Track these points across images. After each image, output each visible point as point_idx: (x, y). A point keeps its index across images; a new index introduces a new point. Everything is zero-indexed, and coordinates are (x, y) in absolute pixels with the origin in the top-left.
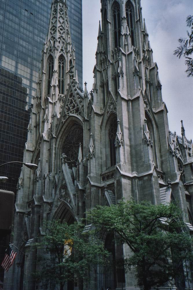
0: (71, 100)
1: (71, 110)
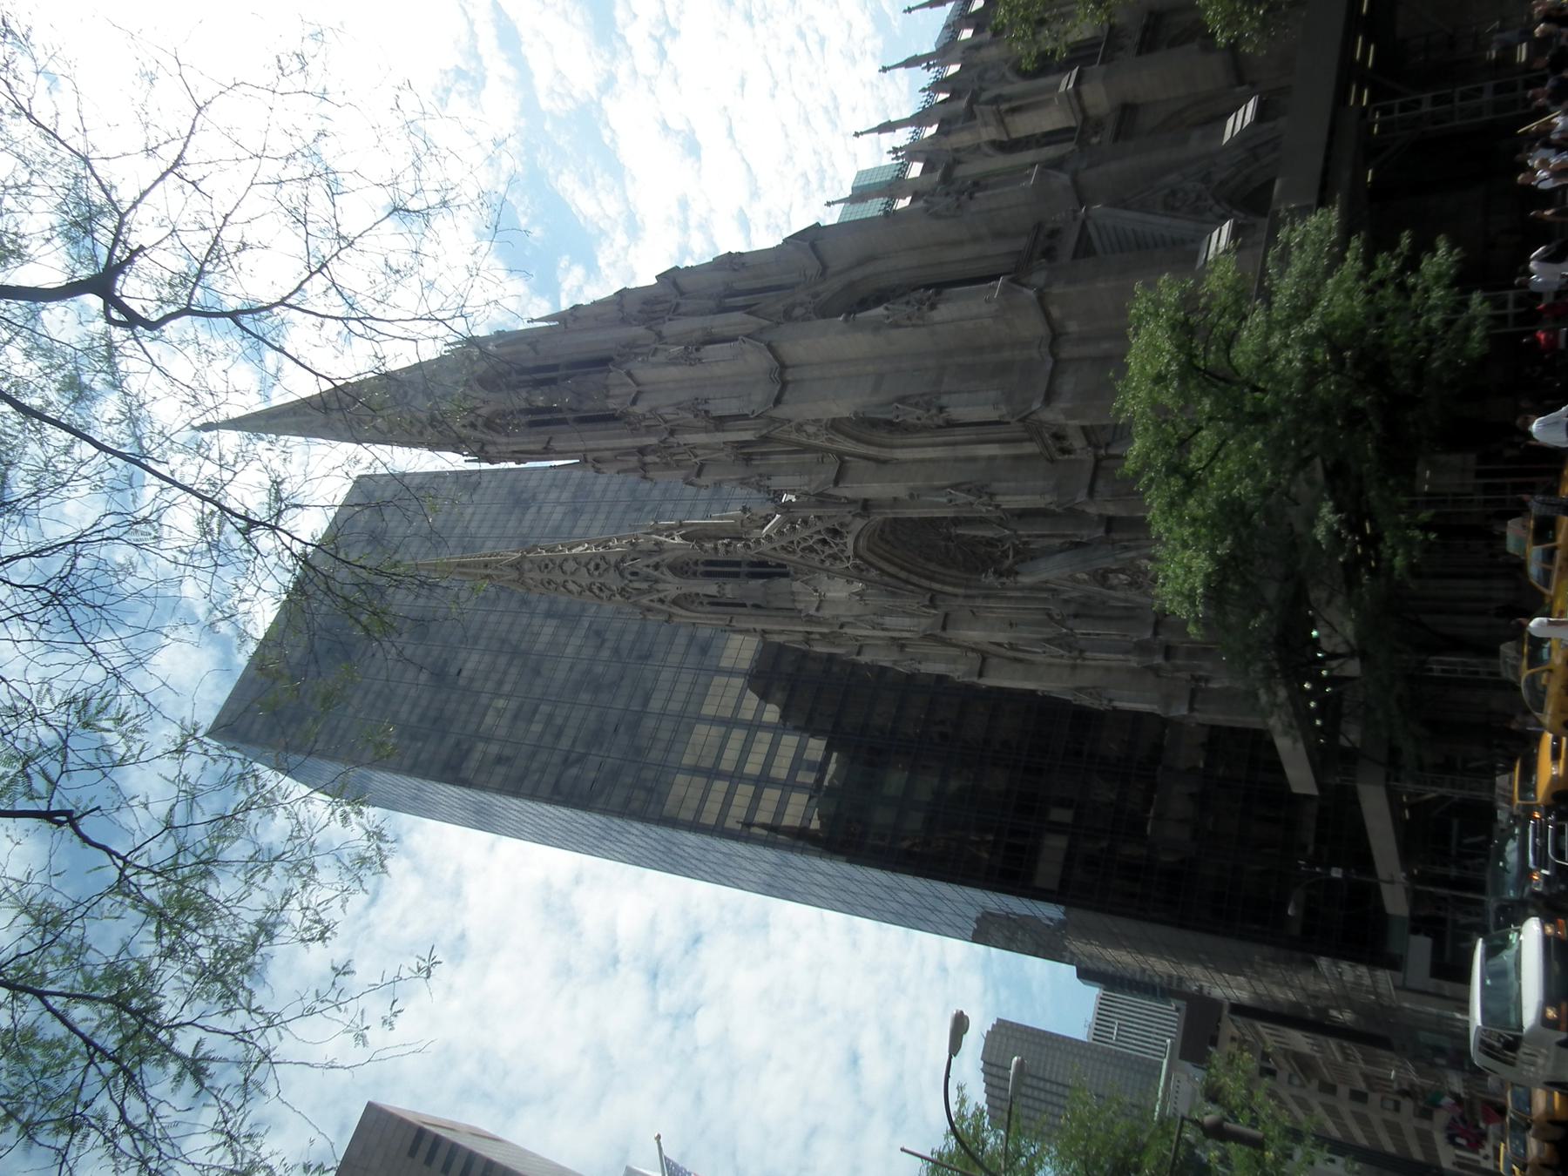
0: (803, 550)
1: (836, 549)
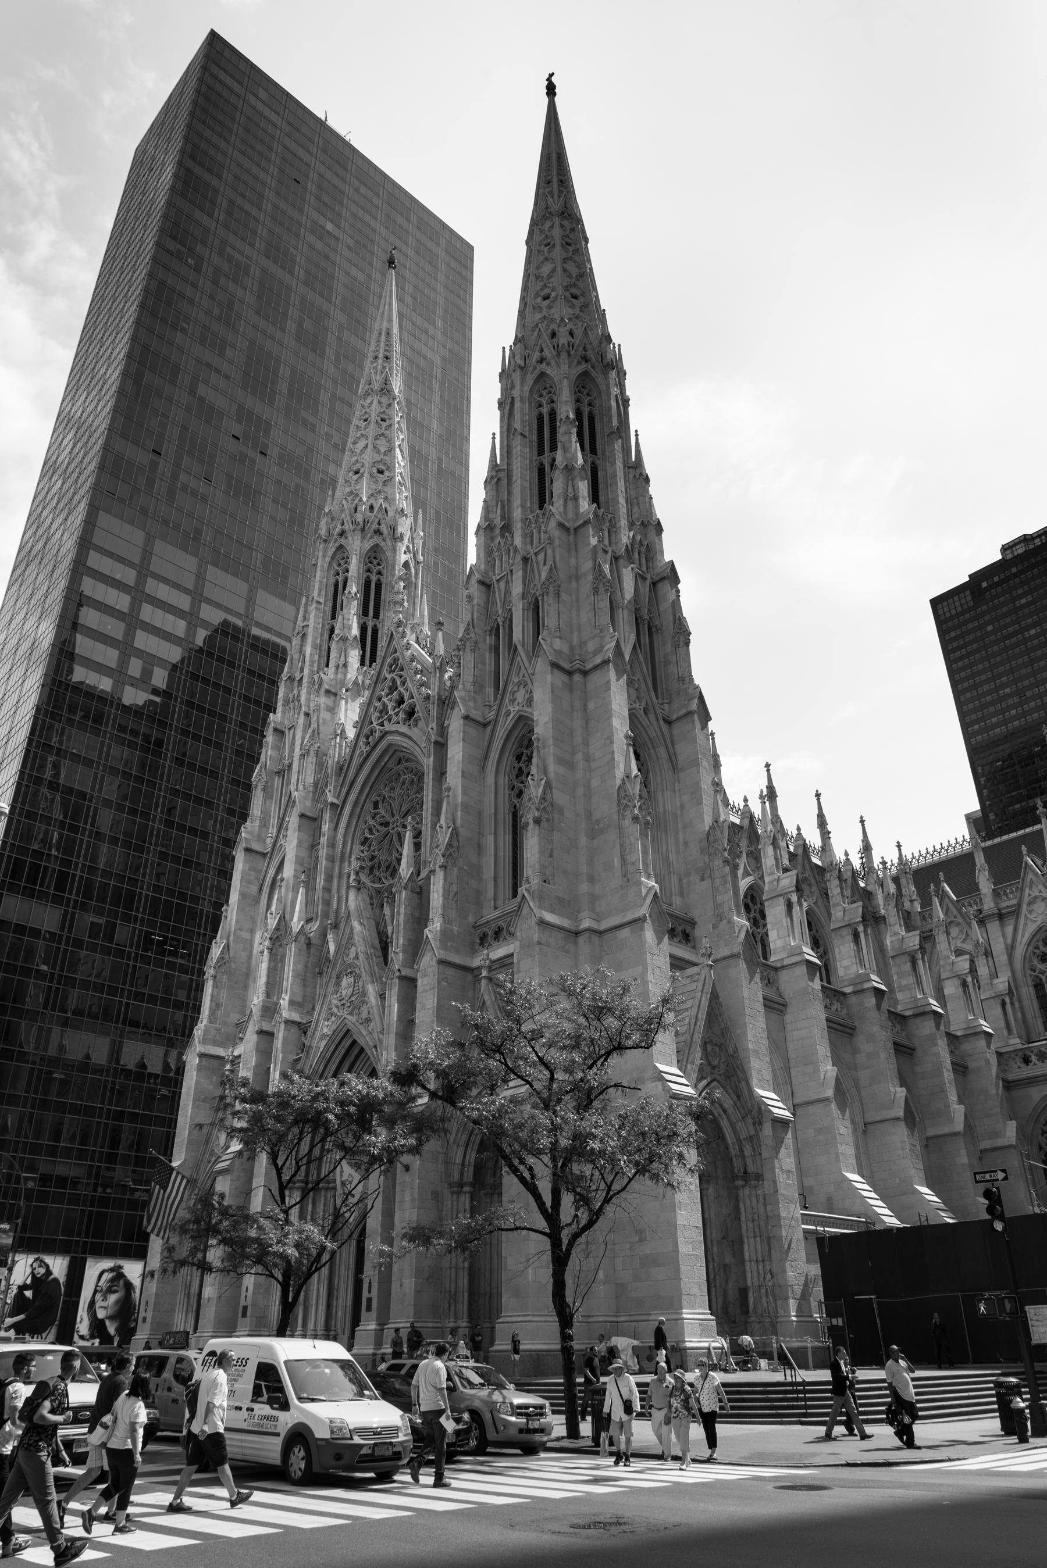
0: (394, 681)
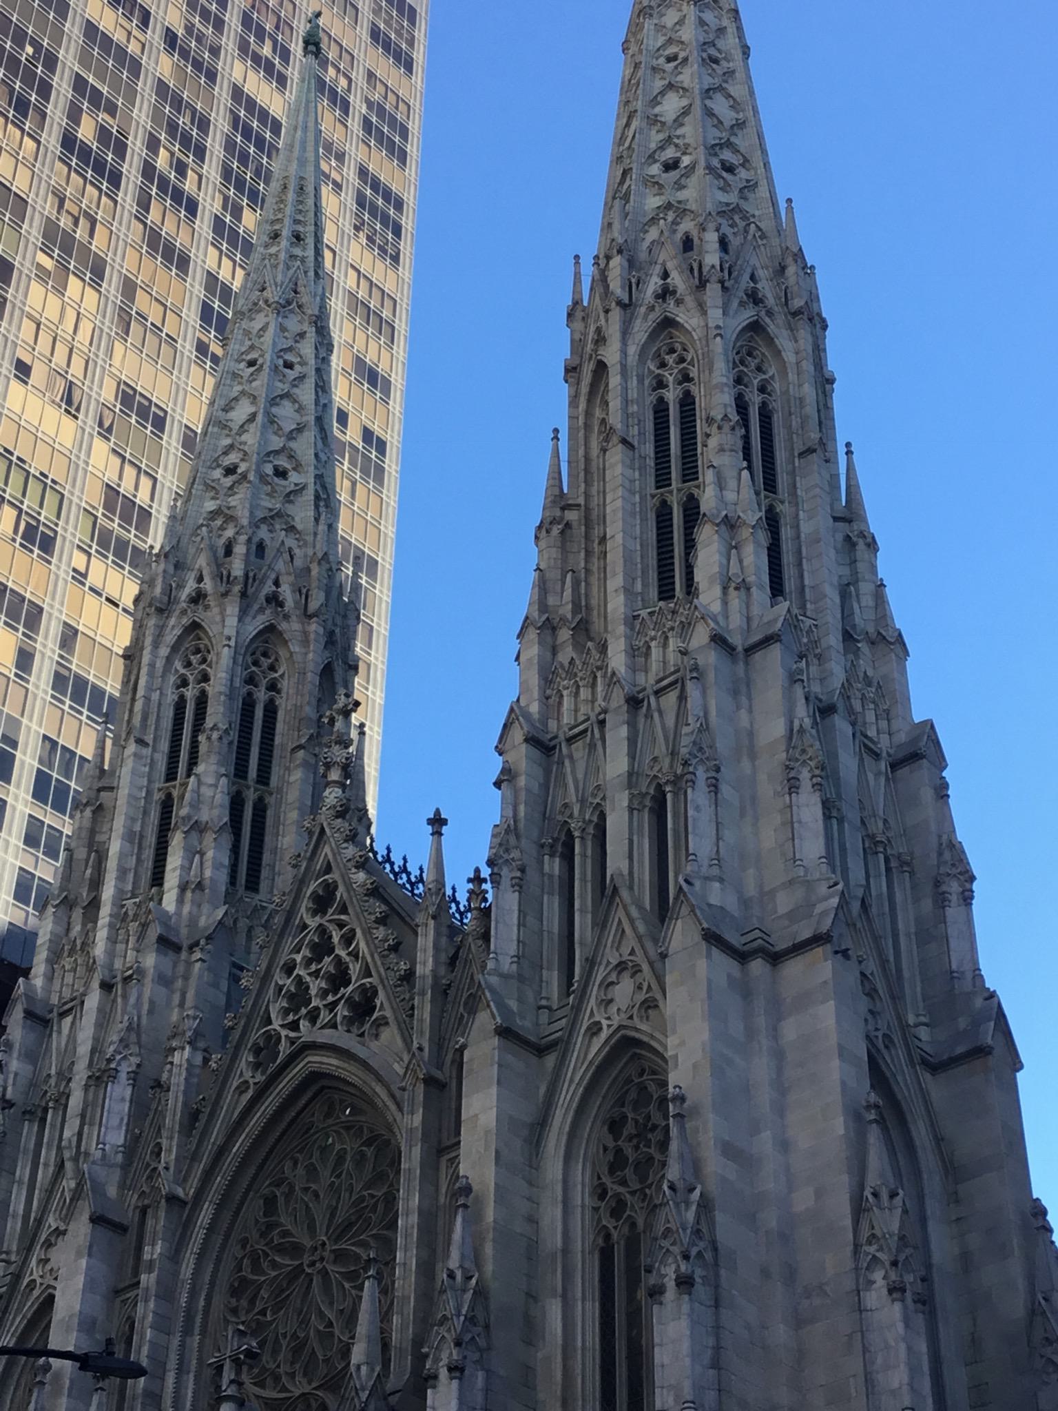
0: (322, 930)
